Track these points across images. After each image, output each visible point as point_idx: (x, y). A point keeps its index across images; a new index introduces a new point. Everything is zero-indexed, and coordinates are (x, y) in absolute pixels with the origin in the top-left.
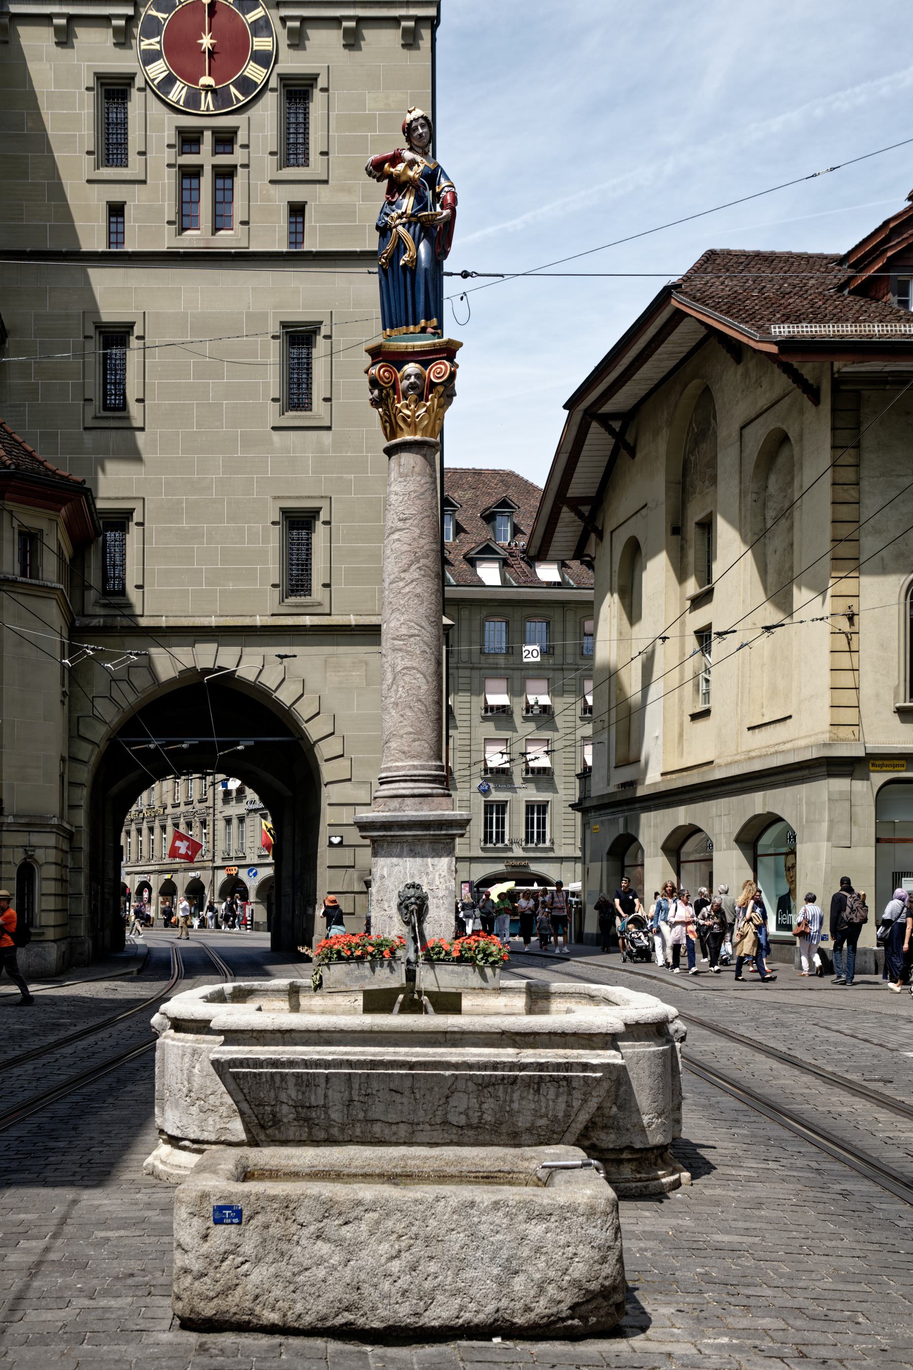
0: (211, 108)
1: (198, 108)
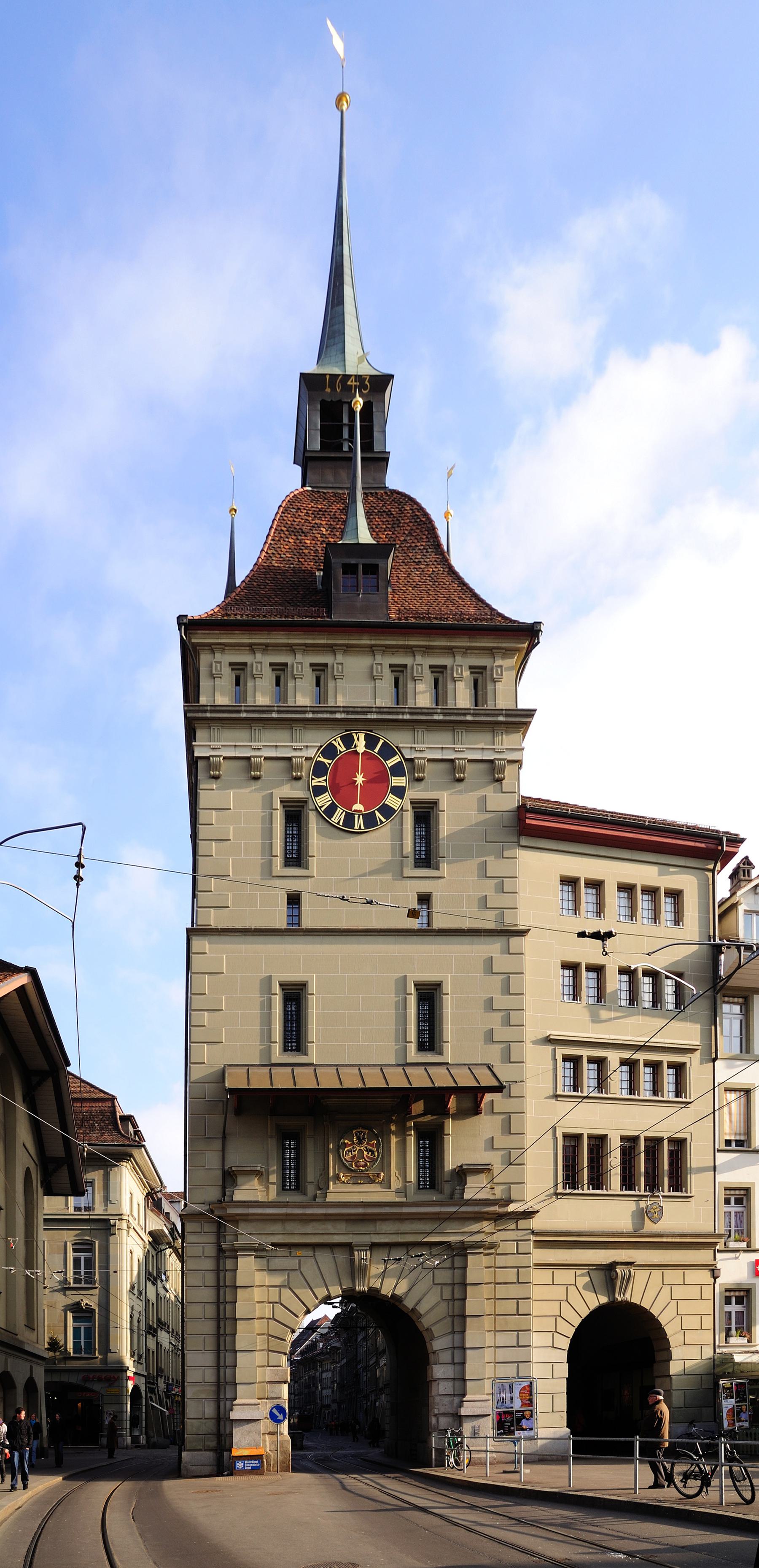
0: (362, 827)
1: (353, 827)
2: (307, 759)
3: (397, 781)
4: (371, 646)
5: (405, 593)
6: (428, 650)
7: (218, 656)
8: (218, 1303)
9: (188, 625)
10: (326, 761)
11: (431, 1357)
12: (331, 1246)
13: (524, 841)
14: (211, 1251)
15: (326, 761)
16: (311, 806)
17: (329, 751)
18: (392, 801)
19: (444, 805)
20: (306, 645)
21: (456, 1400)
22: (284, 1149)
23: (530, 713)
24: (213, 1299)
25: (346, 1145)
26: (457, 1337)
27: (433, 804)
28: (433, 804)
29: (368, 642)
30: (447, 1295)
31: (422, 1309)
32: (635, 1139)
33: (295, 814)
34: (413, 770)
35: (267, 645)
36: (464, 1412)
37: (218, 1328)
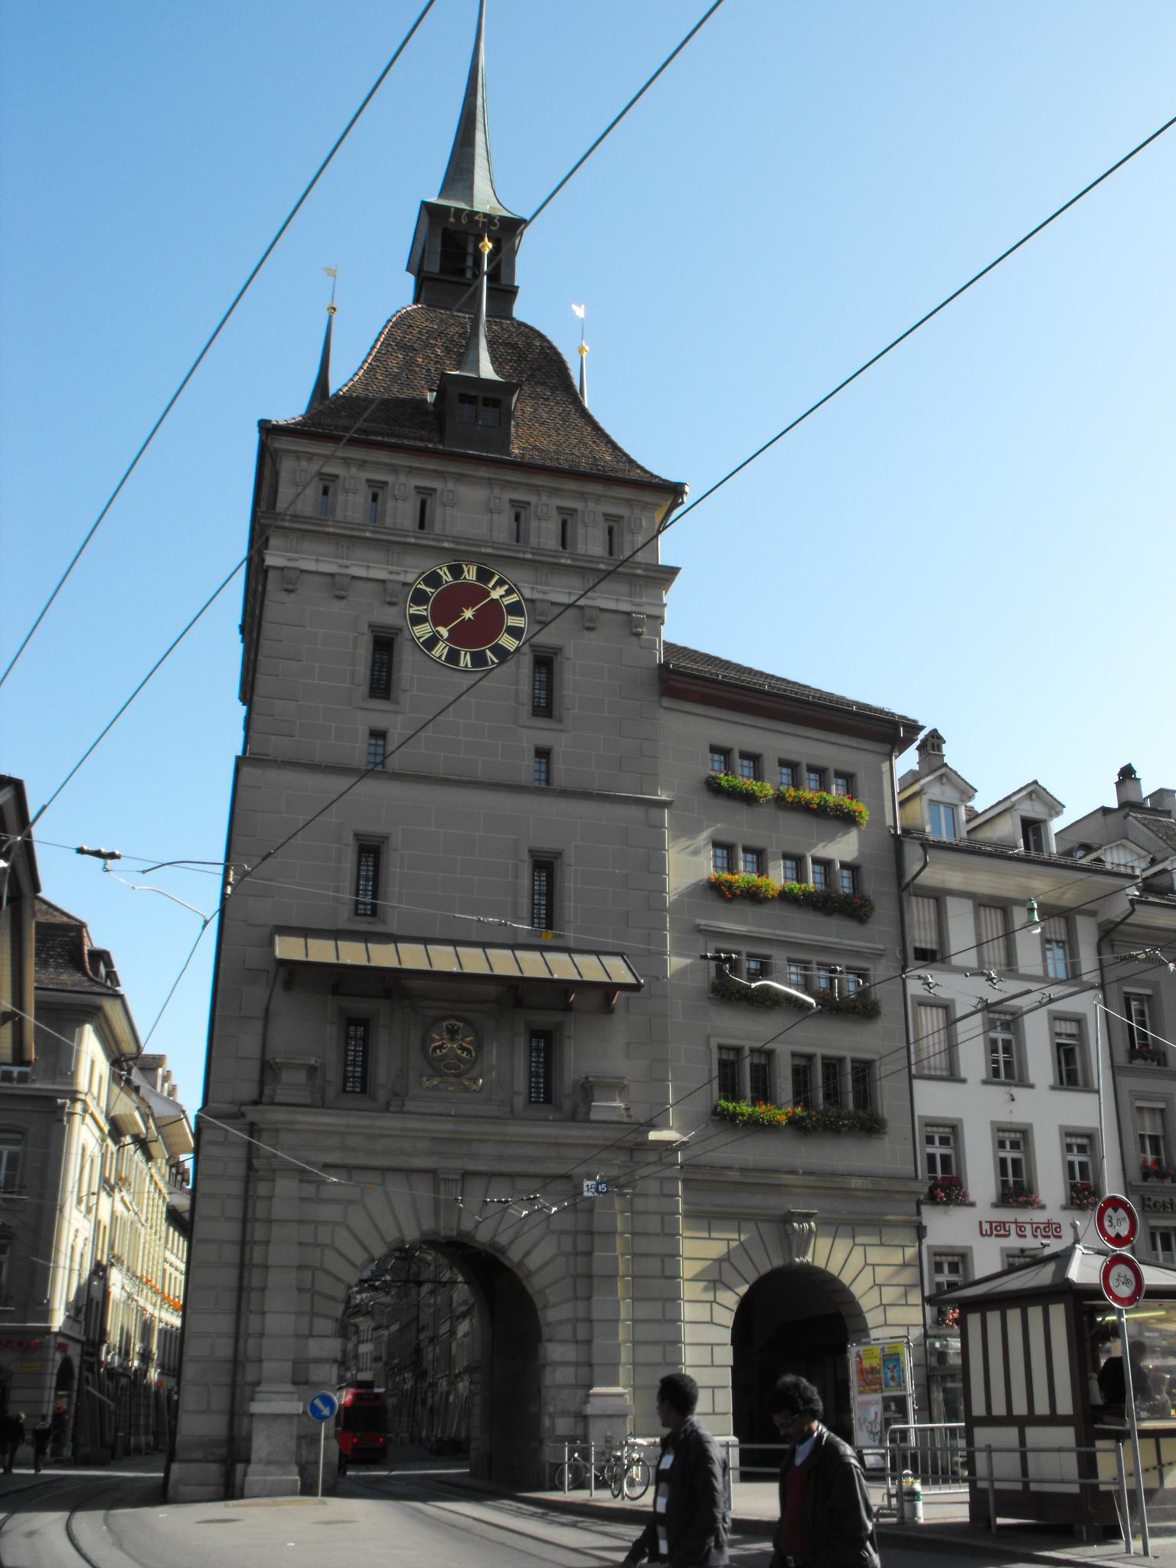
1: (457, 663)
2: (404, 584)
3: (512, 621)
4: (490, 479)
5: (529, 434)
6: (555, 492)
7: (304, 464)
8: (243, 1243)
9: (267, 429)
10: (428, 590)
11: (546, 1332)
12: (408, 1172)
13: (666, 702)
14: (239, 1170)
15: (428, 590)
16: (406, 635)
17: (433, 579)
18: (508, 642)
19: (570, 651)
20: (411, 468)
21: (580, 1393)
22: (348, 1037)
23: (673, 572)
24: (237, 1237)
25: (434, 1040)
26: (581, 1305)
27: (558, 650)
28: (558, 650)
29: (486, 475)
30: (567, 1244)
31: (534, 1262)
32: (810, 1057)
33: (384, 644)
34: (533, 612)
35: (364, 462)
36: (589, 1410)
37: (241, 1278)
